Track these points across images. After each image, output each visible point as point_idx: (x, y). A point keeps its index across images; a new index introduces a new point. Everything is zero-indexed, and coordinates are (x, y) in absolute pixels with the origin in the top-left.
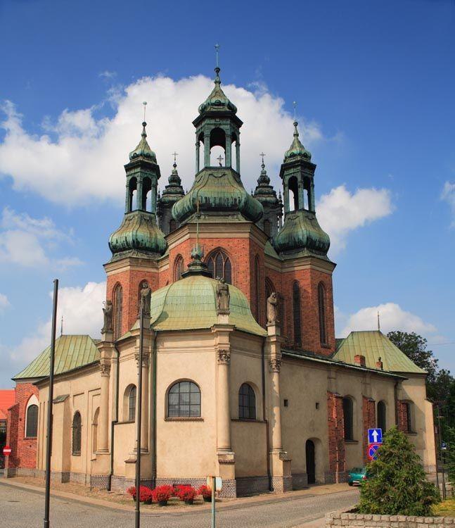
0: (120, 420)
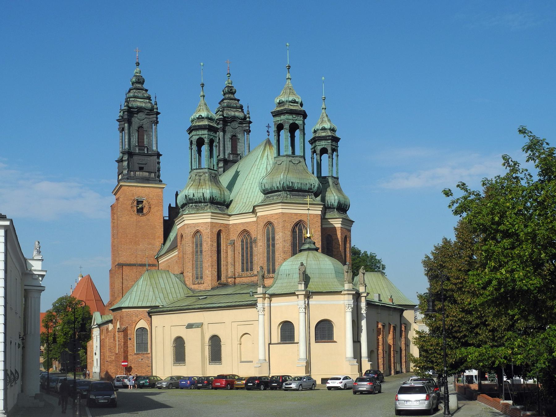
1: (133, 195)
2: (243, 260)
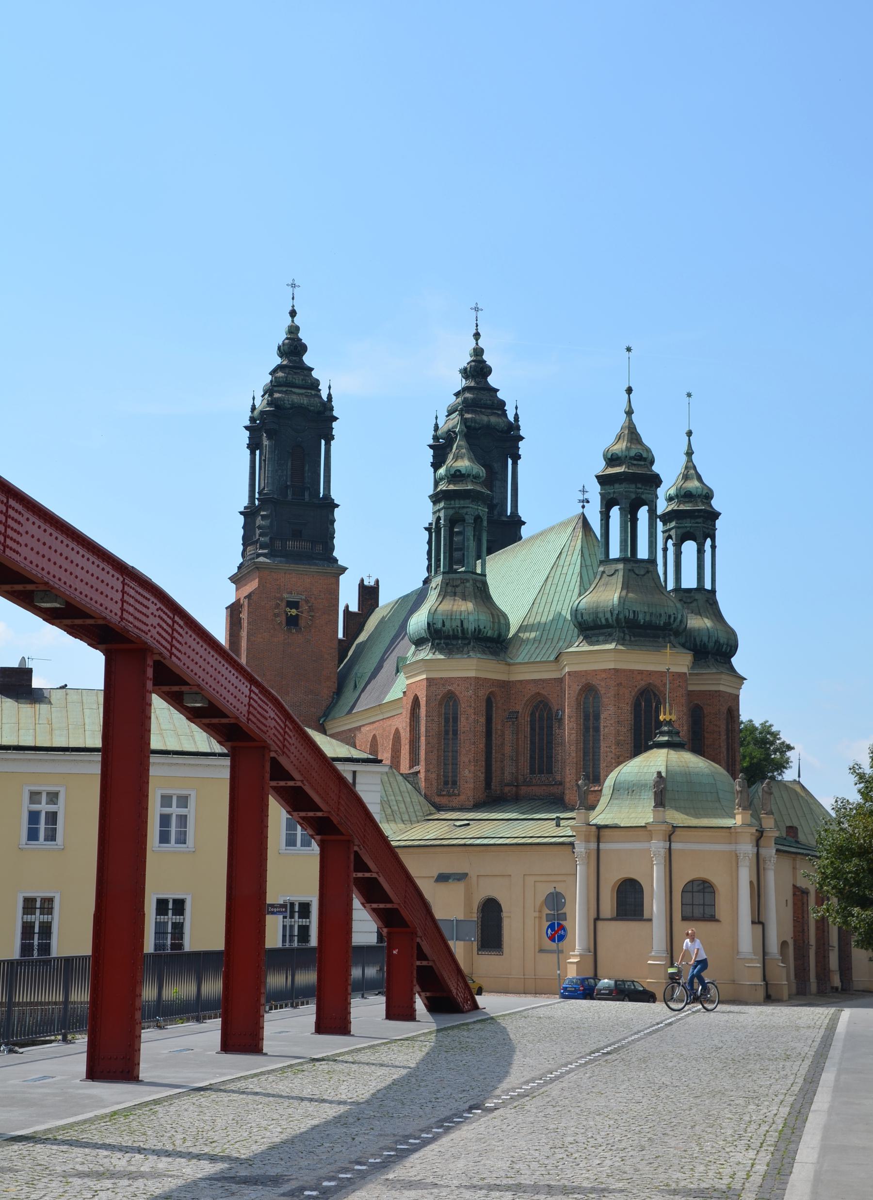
0: (602, 916)
2: (533, 751)
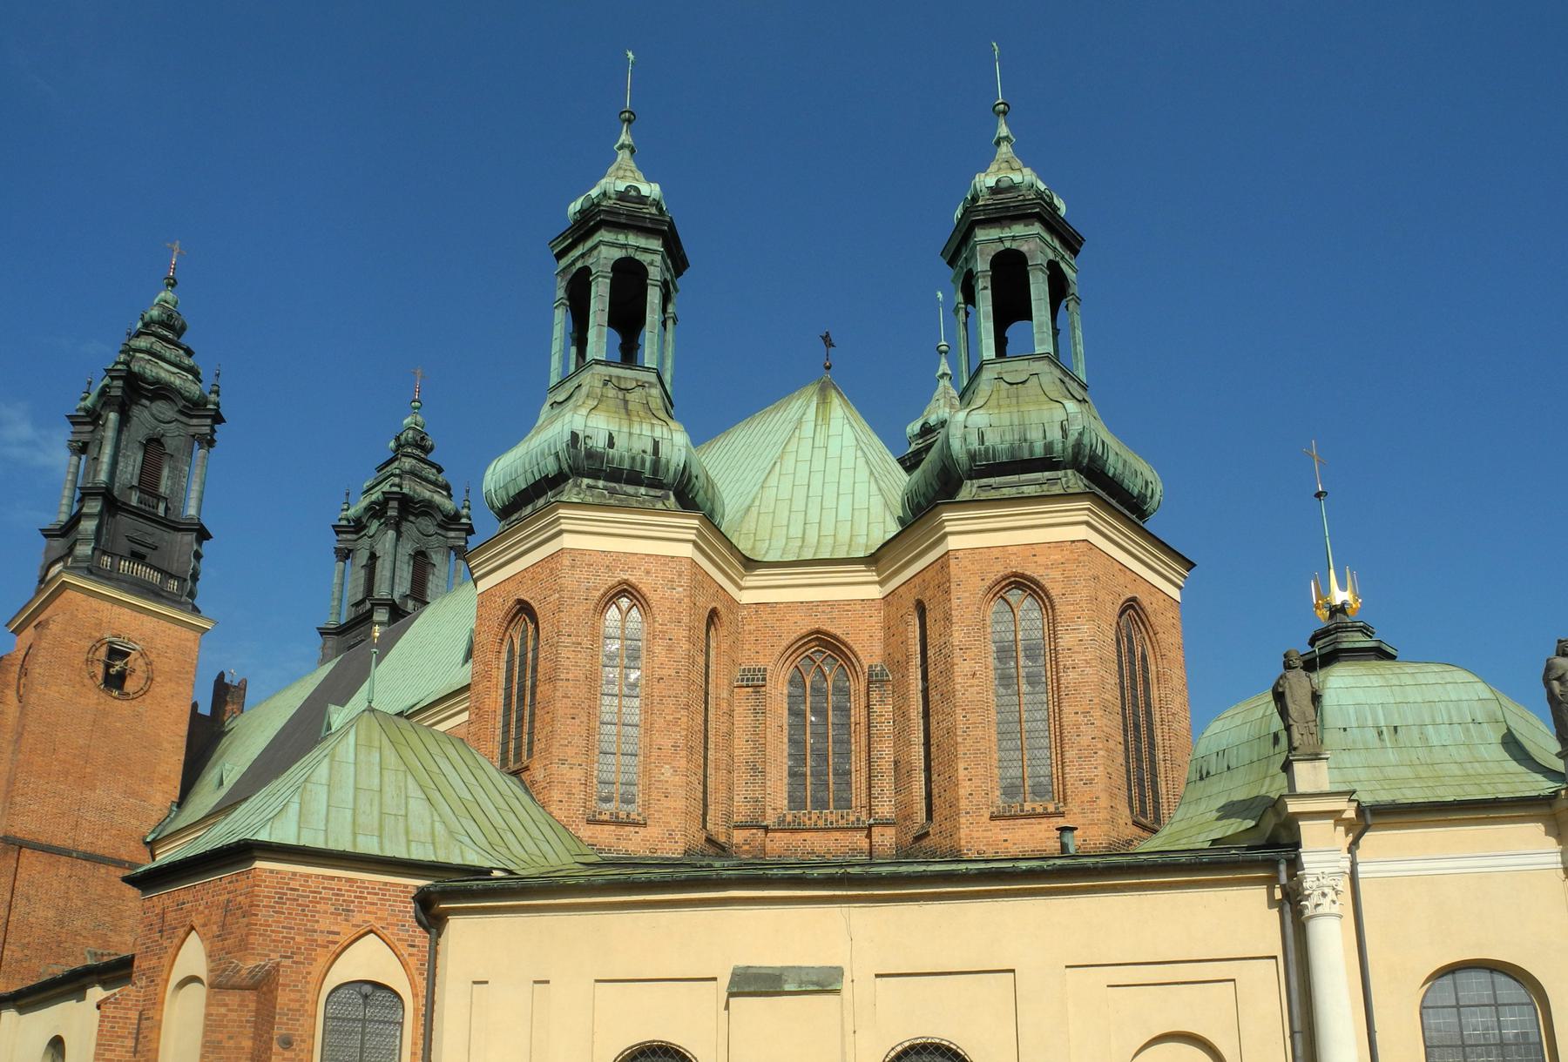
1: (99, 625)
